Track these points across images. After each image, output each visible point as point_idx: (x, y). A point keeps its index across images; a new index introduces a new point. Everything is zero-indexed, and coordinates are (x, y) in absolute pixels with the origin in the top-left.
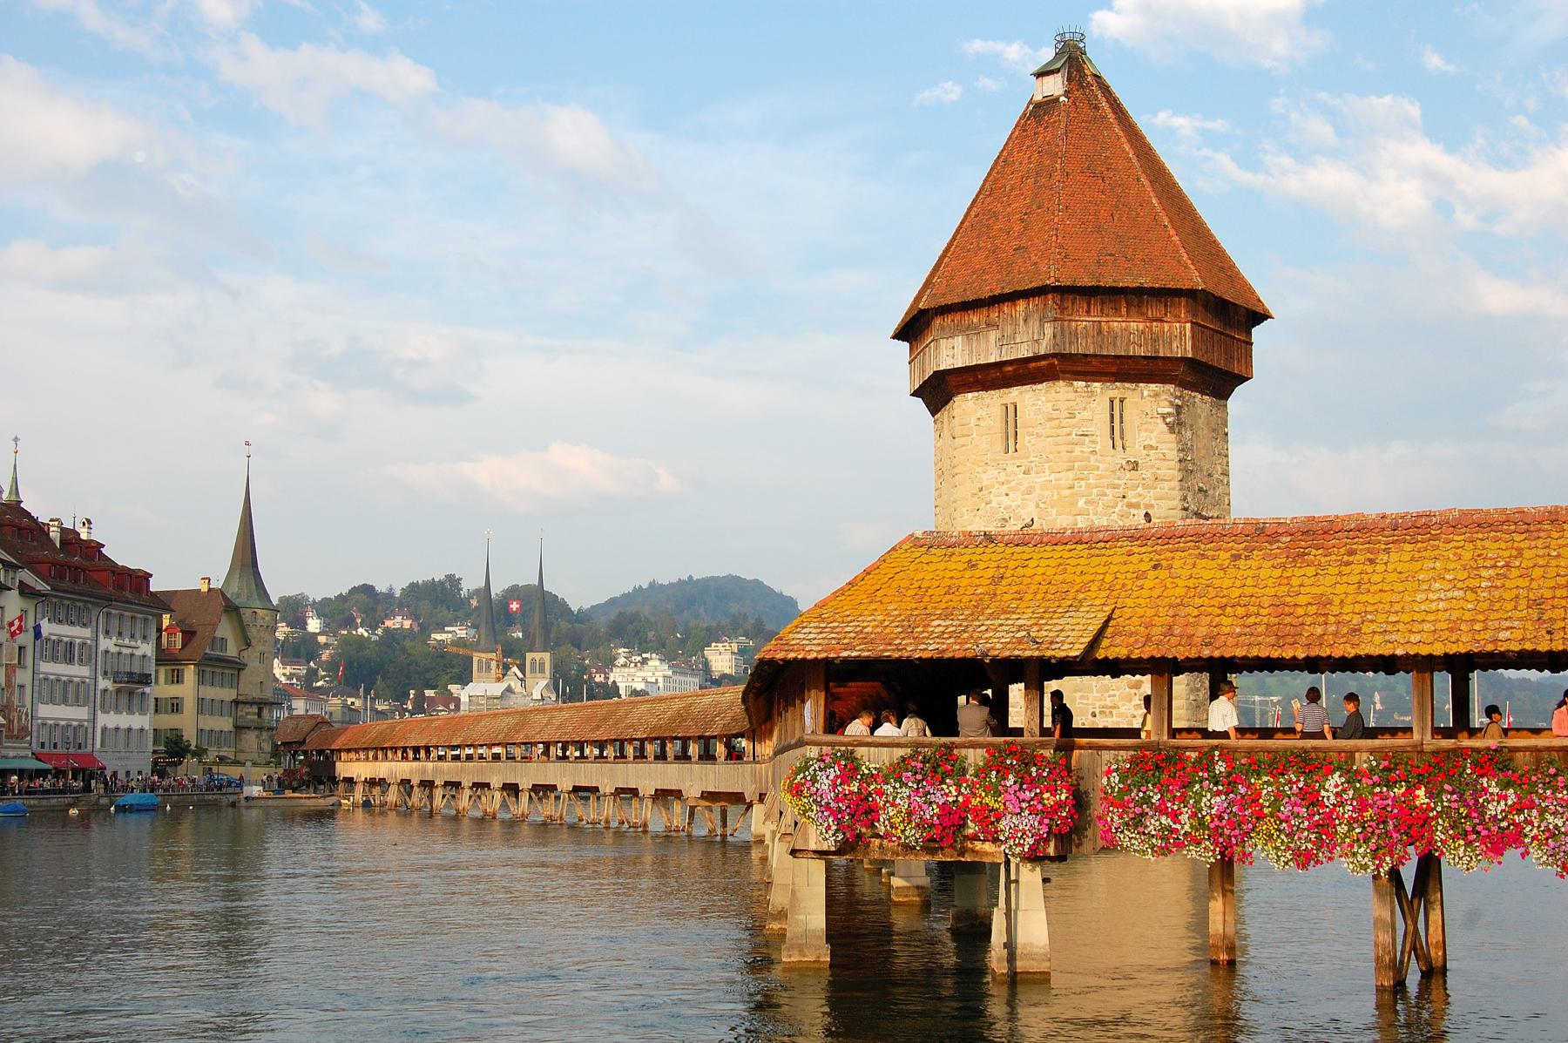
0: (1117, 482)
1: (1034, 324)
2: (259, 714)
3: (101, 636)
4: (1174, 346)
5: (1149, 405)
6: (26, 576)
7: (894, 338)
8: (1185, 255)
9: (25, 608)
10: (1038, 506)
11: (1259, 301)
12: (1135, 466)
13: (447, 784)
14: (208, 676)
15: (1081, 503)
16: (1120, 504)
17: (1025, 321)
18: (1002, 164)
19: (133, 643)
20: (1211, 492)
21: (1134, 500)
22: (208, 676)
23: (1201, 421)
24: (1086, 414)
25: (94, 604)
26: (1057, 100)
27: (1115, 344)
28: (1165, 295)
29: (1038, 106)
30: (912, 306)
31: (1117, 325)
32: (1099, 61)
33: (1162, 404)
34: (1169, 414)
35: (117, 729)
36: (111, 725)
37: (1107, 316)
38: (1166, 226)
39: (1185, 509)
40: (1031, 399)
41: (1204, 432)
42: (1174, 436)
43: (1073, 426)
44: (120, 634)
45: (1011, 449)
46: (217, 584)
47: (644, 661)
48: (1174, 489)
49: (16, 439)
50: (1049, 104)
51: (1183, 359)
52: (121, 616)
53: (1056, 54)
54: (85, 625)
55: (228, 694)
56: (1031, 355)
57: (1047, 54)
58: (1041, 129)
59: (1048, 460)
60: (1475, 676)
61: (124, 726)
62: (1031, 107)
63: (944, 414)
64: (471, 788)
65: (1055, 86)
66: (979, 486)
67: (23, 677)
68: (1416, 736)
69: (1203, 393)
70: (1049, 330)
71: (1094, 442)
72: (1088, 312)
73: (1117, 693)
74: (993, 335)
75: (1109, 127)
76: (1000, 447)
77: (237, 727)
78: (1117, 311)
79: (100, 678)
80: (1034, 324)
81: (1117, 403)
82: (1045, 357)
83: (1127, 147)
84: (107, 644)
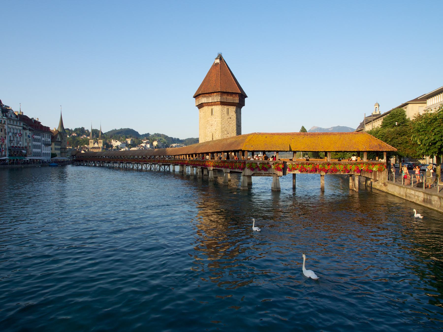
2: (65, 151)
14: (56, 144)
17: (216, 96)
18: (210, 72)
22: (56, 144)
24: (224, 110)
26: (219, 63)
29: (216, 64)
31: (228, 97)
32: (224, 57)
35: (45, 153)
36: (44, 152)
46: (56, 129)
47: (116, 142)
49: (20, 104)
50: (217, 64)
54: (40, 136)
55: (59, 147)
61: (46, 153)
63: (202, 109)
65: (218, 61)
70: (219, 98)
74: (211, 98)
76: (211, 114)
77: (61, 153)
80: (217, 97)
84: (43, 139)
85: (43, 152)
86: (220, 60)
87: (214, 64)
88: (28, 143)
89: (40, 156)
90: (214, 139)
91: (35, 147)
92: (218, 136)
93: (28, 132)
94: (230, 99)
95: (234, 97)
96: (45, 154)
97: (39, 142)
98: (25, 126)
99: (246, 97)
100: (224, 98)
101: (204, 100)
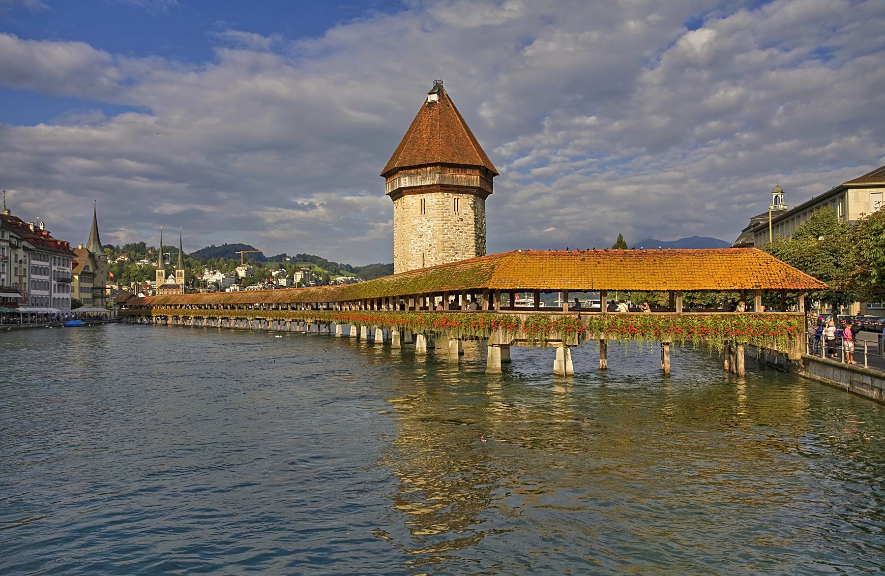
2: (102, 293)
3: (53, 265)
5: (466, 201)
6: (25, 243)
9: (25, 255)
12: (462, 220)
14: (83, 279)
15: (446, 231)
17: (430, 173)
24: (448, 203)
25: (50, 254)
26: (436, 102)
28: (473, 167)
32: (447, 90)
39: (476, 234)
40: (431, 199)
44: (59, 264)
47: (215, 273)
50: (434, 103)
54: (47, 261)
55: (90, 285)
59: (436, 217)
61: (61, 297)
67: (25, 280)
70: (438, 176)
74: (419, 177)
75: (453, 112)
76: (420, 212)
77: (93, 297)
79: (52, 280)
80: (432, 174)
81: (456, 200)
82: (436, 184)
83: (458, 119)
84: (54, 268)
85: (53, 297)
86: (438, 95)
87: (425, 103)
88: (21, 277)
89: (47, 306)
90: (427, 266)
91: (37, 285)
92: (436, 259)
93: (21, 253)
94: (461, 178)
95: (471, 175)
96: (57, 302)
97: (45, 274)
98: (14, 241)
99: (496, 174)
100: (445, 178)
101: (405, 182)
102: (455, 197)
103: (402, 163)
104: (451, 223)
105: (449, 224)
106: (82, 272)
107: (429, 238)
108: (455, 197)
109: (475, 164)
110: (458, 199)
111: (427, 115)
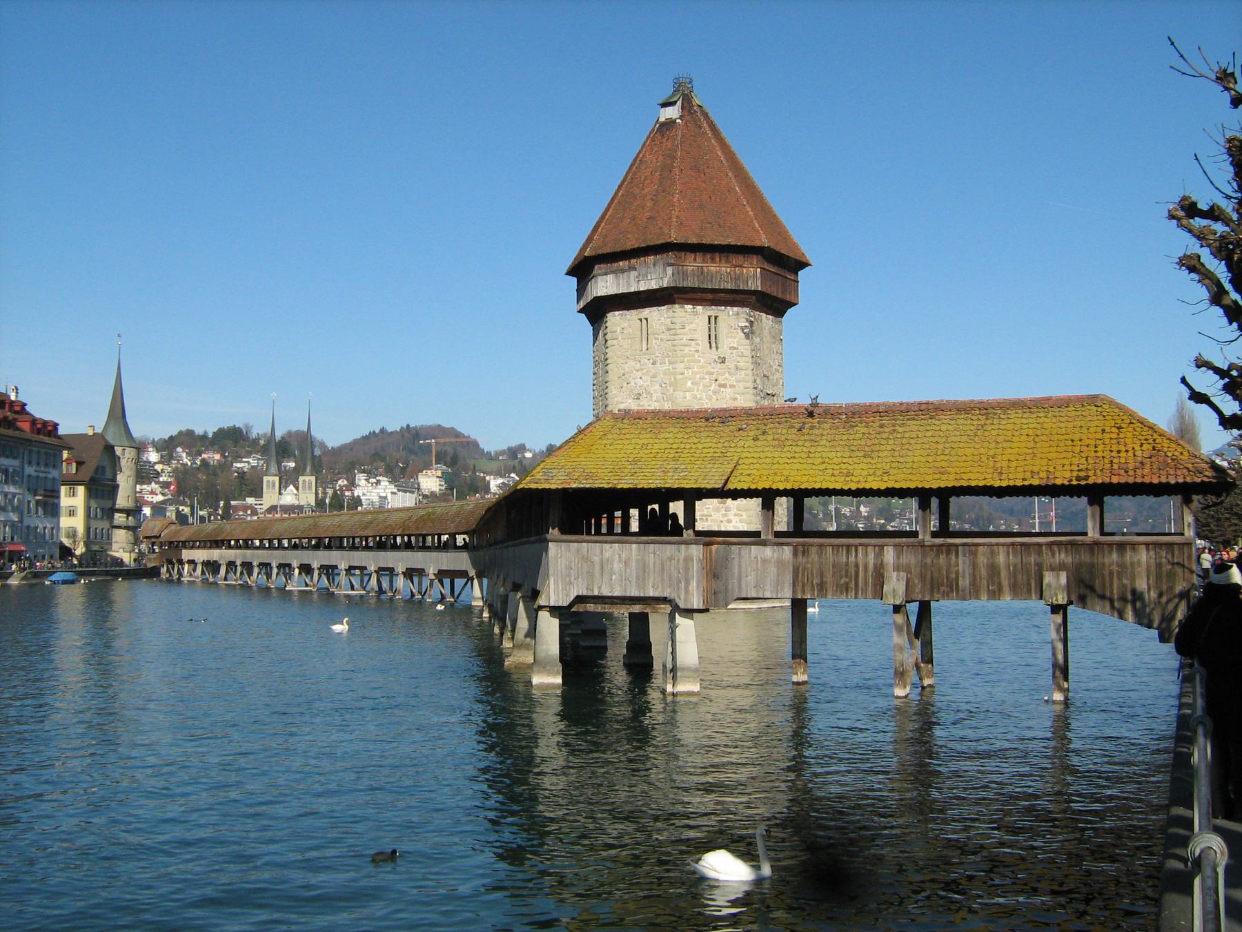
0: (712, 370)
1: (660, 268)
3: (26, 466)
4: (750, 283)
5: (733, 321)
7: (567, 274)
8: (757, 224)
10: (661, 386)
11: (803, 254)
13: (261, 565)
15: (689, 384)
16: (714, 385)
17: (654, 265)
18: (637, 163)
19: (46, 470)
20: (771, 377)
21: (723, 382)
23: (766, 332)
24: (693, 326)
26: (674, 121)
27: (712, 281)
29: (663, 125)
30: (579, 254)
31: (713, 268)
33: (741, 320)
34: (746, 326)
37: (707, 263)
38: (744, 205)
39: (755, 388)
40: (657, 316)
41: (767, 338)
42: (748, 341)
43: (684, 334)
45: (644, 348)
46: (99, 430)
47: (378, 482)
48: (748, 375)
50: (670, 123)
51: (755, 292)
52: (38, 452)
53: (674, 91)
54: (15, 458)
55: (108, 504)
56: (658, 287)
57: (667, 92)
58: (664, 140)
60: (953, 500)
62: (658, 125)
64: (319, 569)
66: (623, 371)
68: (921, 537)
69: (767, 314)
70: (669, 270)
71: (698, 344)
72: (695, 259)
73: (711, 506)
74: (633, 274)
75: (709, 140)
76: (638, 347)
78: (713, 260)
80: (660, 268)
81: (713, 320)
82: (667, 288)
84: (30, 470)
94: (720, 273)
95: (741, 266)
99: (803, 265)
101: (605, 285)
102: (710, 313)
103: (600, 248)
104: (702, 367)
105: (695, 370)
106: (92, 479)
107: (654, 399)
108: (710, 313)
109: (748, 243)
110: (716, 318)
111: (656, 149)
